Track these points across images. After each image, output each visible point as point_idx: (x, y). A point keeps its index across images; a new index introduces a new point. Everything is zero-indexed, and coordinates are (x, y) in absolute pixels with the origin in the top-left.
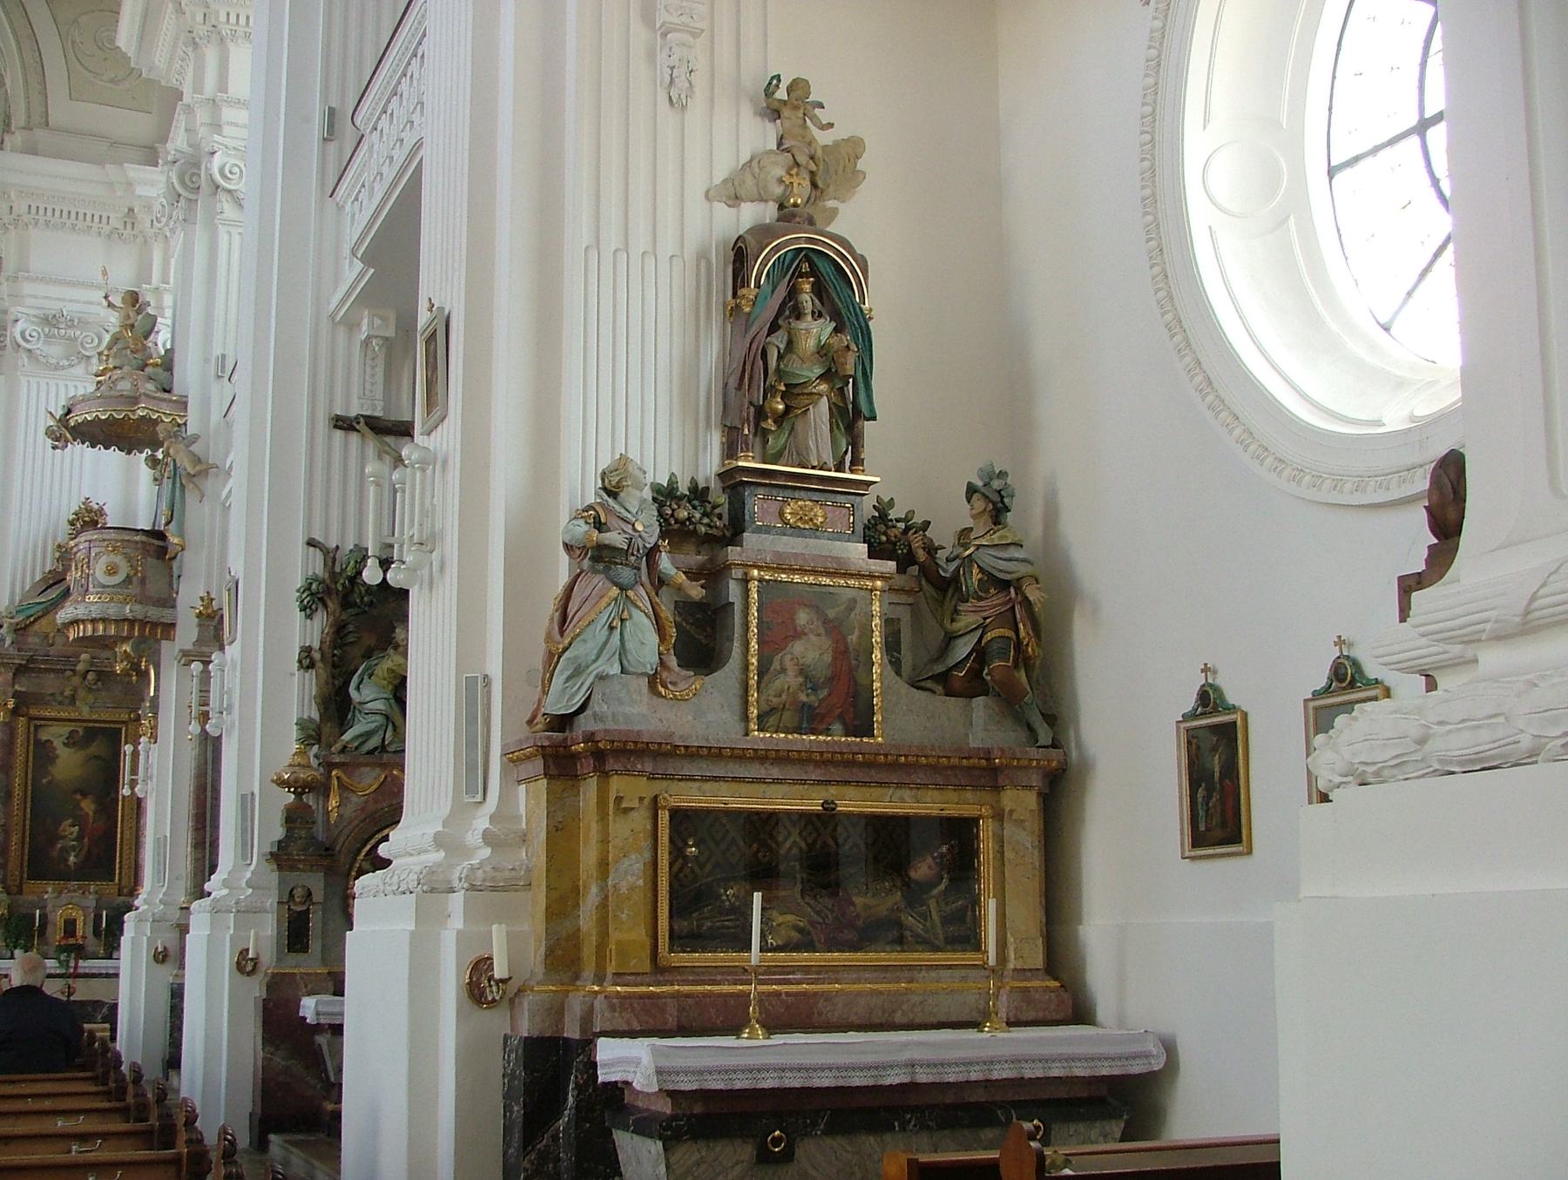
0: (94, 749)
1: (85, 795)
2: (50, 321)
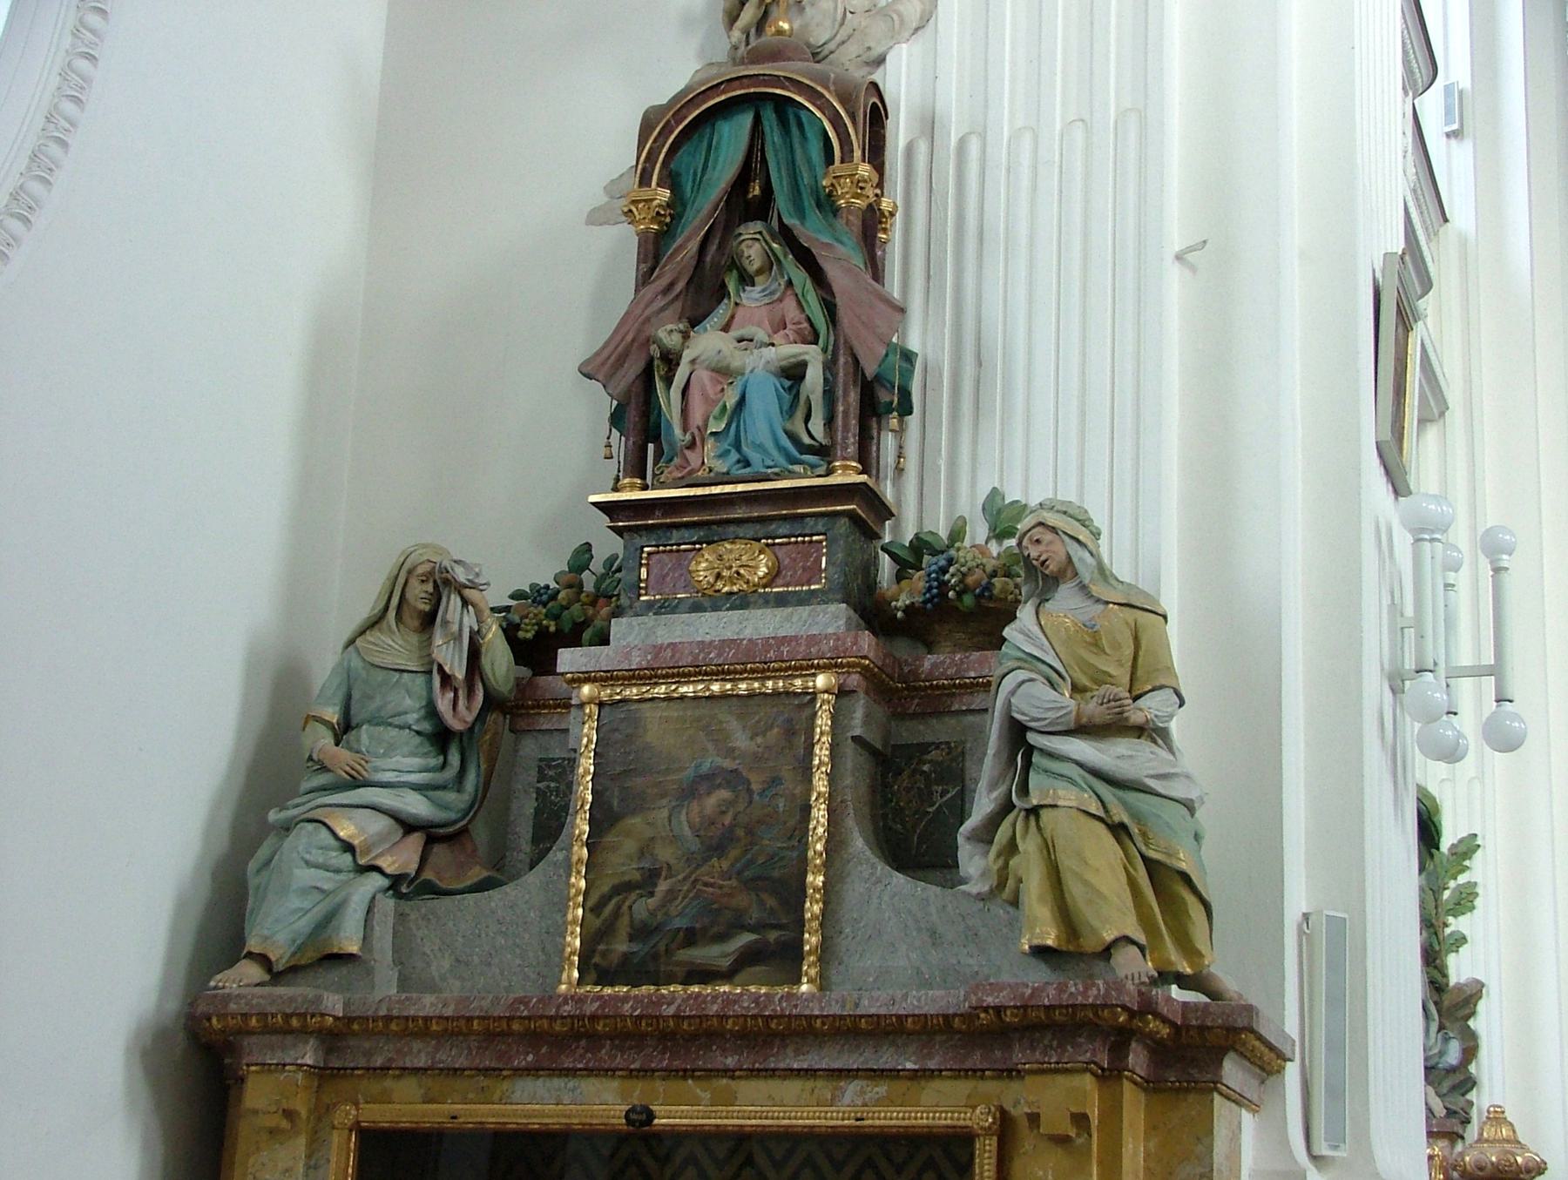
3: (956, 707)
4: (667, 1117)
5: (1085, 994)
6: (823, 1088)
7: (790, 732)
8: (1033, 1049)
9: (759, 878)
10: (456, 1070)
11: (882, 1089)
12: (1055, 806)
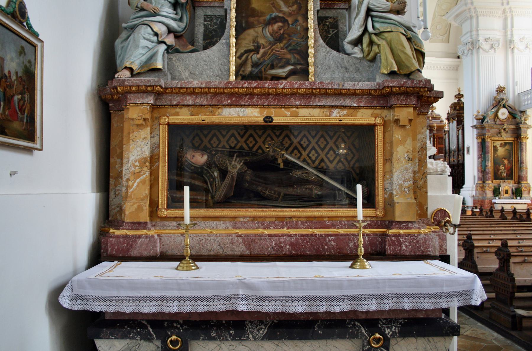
0: (507, 147)
1: (505, 159)
2: (486, 40)
3: (335, 7)
4: (277, 120)
5: (419, 84)
6: (327, 111)
7: (300, 8)
8: (398, 100)
9: (294, 50)
10: (202, 105)
11: (345, 112)
12: (392, 31)
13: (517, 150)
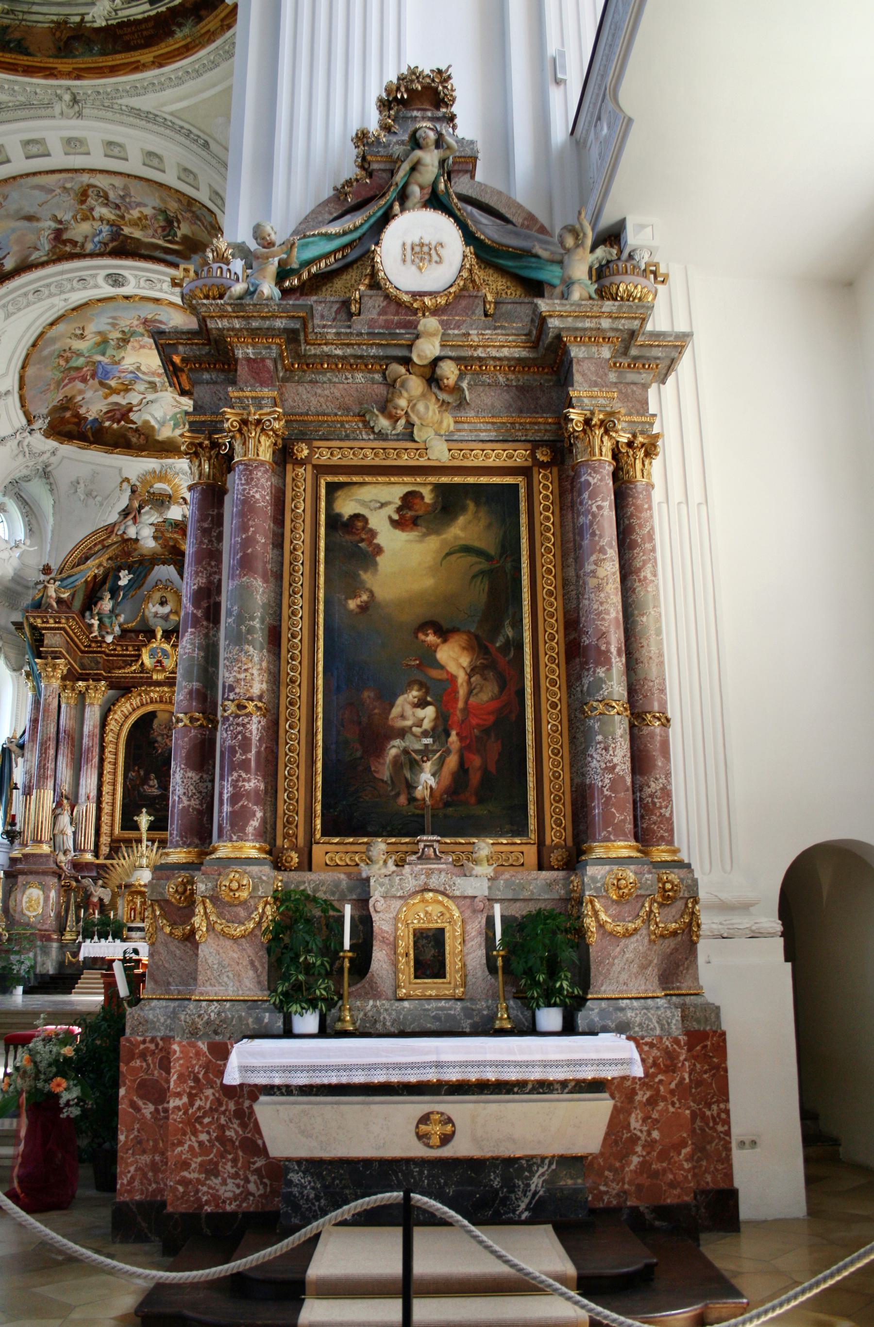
0: (463, 529)
1: (444, 634)
13: (573, 548)
